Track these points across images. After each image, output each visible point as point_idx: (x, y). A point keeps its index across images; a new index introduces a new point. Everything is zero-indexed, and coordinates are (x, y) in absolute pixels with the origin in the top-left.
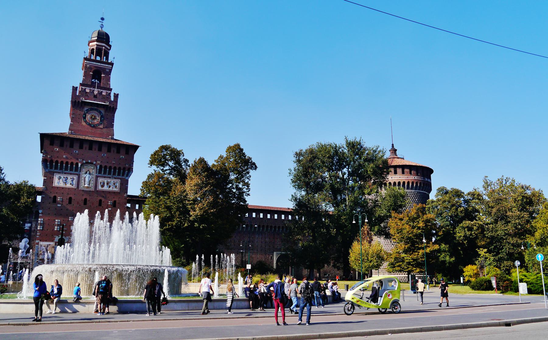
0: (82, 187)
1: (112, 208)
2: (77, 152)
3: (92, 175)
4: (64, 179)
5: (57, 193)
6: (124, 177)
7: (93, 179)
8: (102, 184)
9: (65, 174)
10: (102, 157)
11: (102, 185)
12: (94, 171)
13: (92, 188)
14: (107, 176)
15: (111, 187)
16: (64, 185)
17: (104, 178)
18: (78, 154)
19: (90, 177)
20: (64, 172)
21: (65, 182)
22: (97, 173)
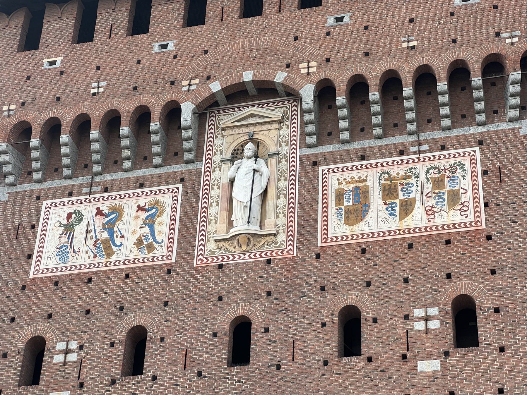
0: (211, 246)
1: (447, 354)
2: (170, 47)
3: (273, 161)
4: (100, 221)
5: (50, 316)
6: (504, 126)
7: (283, 184)
8: (348, 202)
9: (106, 190)
10: (328, 34)
11: (348, 212)
12: (285, 131)
13: (281, 237)
14: (378, 143)
15: (418, 210)
16: (99, 260)
17: (363, 158)
18: (175, 57)
19: (265, 170)
20: (99, 184)
21: (105, 235)
22: (312, 140)
